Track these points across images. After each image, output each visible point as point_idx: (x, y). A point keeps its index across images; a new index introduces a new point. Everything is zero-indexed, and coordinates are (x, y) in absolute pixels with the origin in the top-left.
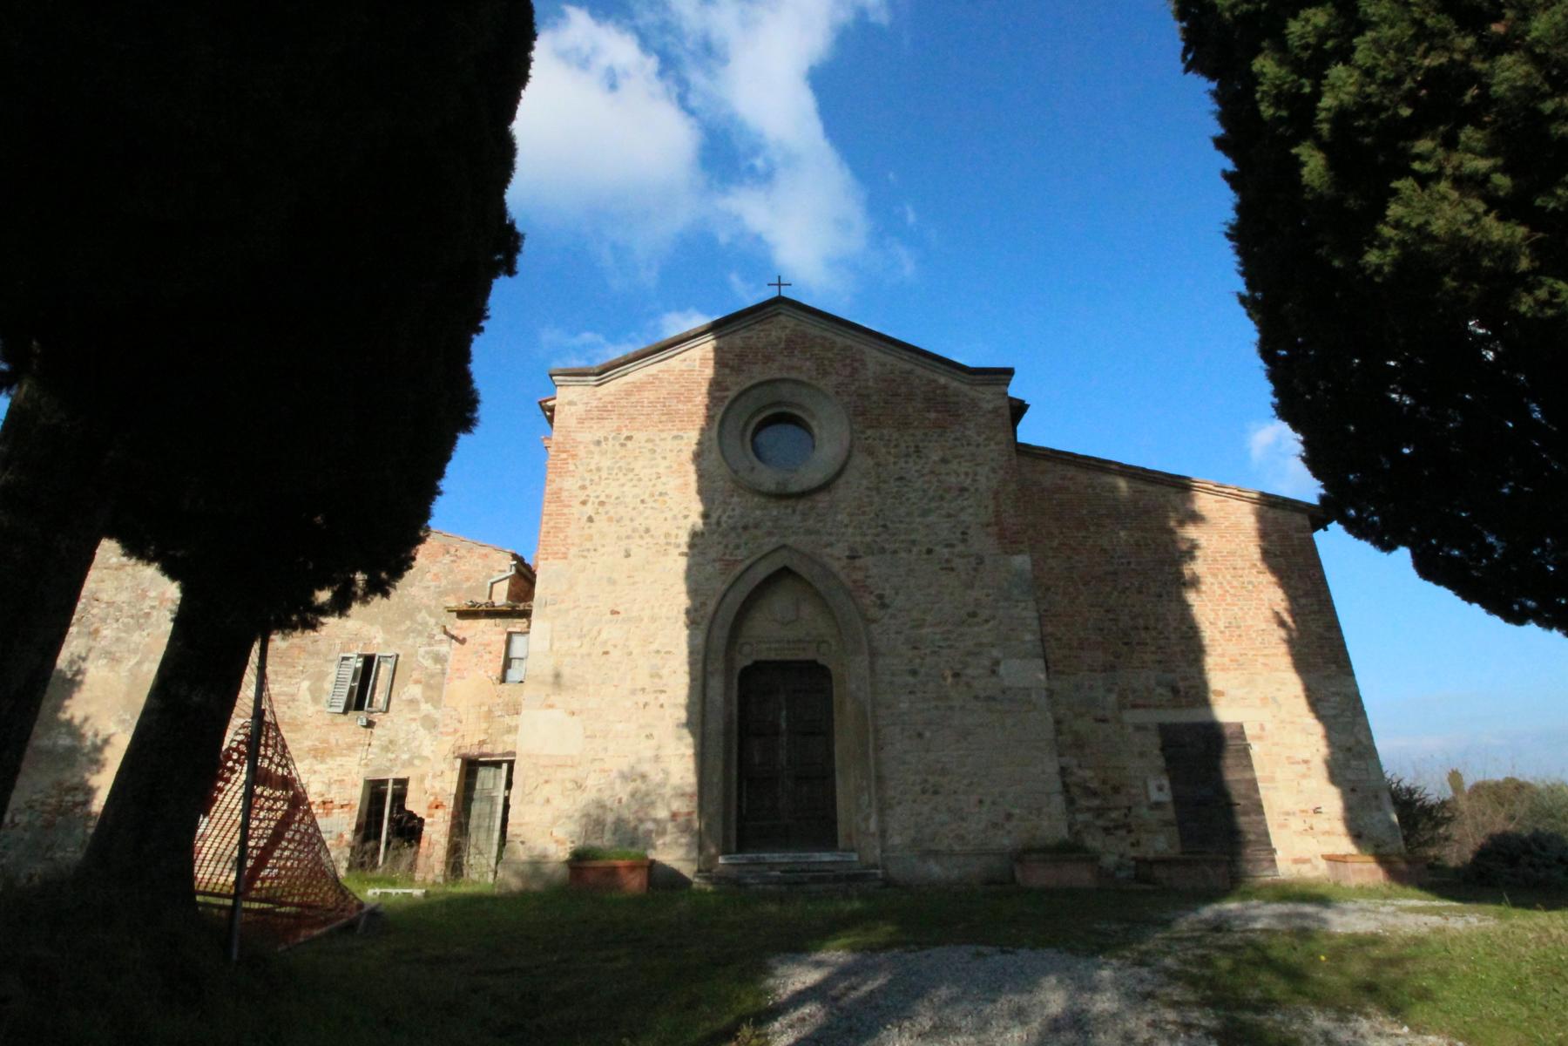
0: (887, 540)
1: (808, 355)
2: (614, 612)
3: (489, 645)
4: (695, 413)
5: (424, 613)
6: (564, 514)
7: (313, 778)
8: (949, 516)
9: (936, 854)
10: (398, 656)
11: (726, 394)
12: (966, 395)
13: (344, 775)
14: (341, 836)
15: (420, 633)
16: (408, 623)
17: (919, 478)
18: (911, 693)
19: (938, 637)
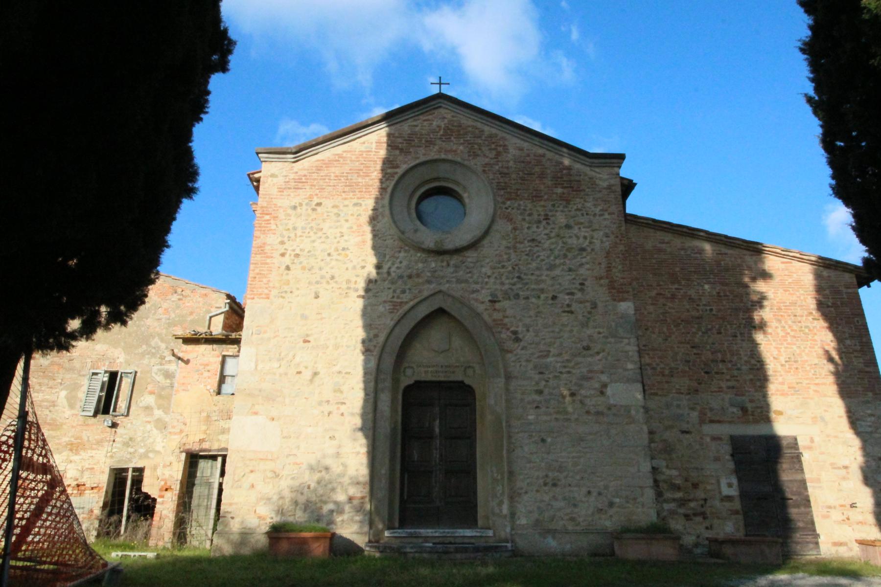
0: (521, 288)
1: (462, 141)
2: (306, 341)
3: (207, 365)
4: (372, 186)
5: (157, 339)
6: (267, 264)
7: (69, 466)
8: (570, 270)
9: (553, 532)
10: (136, 372)
11: (396, 170)
12: (586, 175)
13: (94, 464)
14: (92, 511)
15: (153, 355)
16: (144, 347)
17: (547, 240)
18: (537, 407)
19: (559, 364)
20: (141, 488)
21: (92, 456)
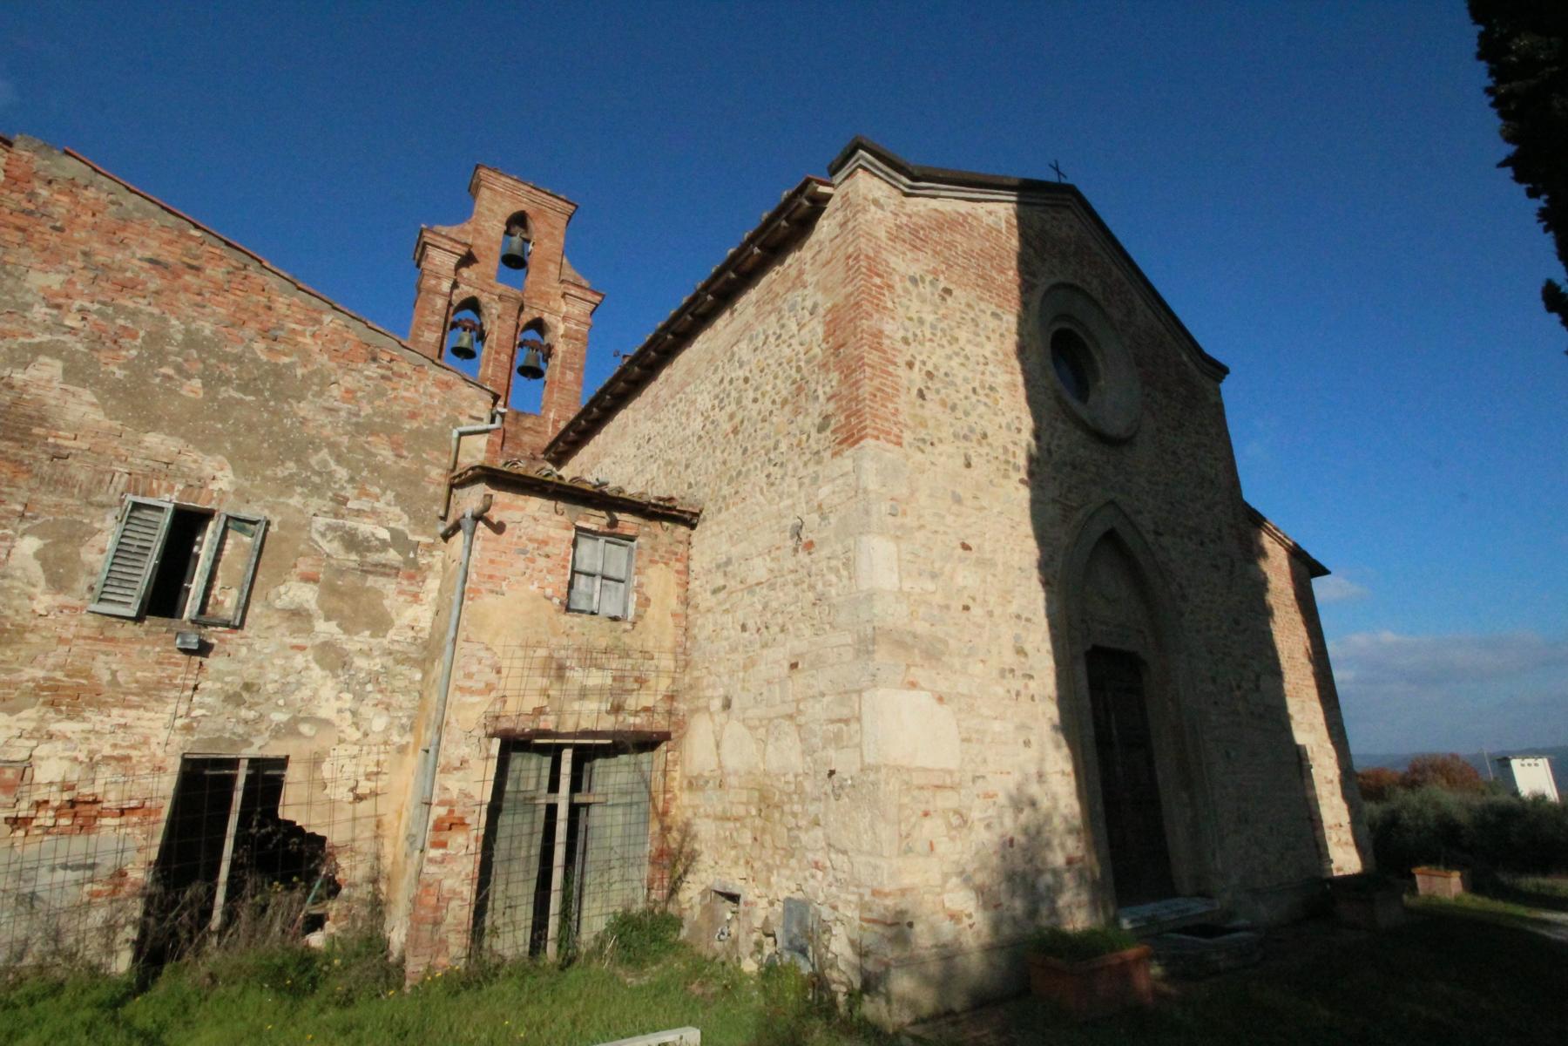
3: (545, 543)
5: (324, 453)
7: (43, 750)
10: (268, 523)
13: (133, 747)
14: (121, 874)
15: (316, 490)
16: (291, 466)
20: (276, 810)
21: (125, 726)
